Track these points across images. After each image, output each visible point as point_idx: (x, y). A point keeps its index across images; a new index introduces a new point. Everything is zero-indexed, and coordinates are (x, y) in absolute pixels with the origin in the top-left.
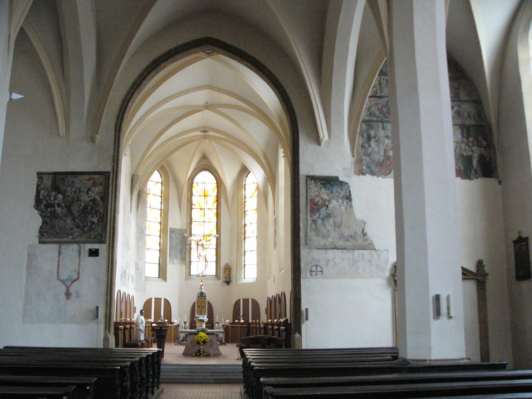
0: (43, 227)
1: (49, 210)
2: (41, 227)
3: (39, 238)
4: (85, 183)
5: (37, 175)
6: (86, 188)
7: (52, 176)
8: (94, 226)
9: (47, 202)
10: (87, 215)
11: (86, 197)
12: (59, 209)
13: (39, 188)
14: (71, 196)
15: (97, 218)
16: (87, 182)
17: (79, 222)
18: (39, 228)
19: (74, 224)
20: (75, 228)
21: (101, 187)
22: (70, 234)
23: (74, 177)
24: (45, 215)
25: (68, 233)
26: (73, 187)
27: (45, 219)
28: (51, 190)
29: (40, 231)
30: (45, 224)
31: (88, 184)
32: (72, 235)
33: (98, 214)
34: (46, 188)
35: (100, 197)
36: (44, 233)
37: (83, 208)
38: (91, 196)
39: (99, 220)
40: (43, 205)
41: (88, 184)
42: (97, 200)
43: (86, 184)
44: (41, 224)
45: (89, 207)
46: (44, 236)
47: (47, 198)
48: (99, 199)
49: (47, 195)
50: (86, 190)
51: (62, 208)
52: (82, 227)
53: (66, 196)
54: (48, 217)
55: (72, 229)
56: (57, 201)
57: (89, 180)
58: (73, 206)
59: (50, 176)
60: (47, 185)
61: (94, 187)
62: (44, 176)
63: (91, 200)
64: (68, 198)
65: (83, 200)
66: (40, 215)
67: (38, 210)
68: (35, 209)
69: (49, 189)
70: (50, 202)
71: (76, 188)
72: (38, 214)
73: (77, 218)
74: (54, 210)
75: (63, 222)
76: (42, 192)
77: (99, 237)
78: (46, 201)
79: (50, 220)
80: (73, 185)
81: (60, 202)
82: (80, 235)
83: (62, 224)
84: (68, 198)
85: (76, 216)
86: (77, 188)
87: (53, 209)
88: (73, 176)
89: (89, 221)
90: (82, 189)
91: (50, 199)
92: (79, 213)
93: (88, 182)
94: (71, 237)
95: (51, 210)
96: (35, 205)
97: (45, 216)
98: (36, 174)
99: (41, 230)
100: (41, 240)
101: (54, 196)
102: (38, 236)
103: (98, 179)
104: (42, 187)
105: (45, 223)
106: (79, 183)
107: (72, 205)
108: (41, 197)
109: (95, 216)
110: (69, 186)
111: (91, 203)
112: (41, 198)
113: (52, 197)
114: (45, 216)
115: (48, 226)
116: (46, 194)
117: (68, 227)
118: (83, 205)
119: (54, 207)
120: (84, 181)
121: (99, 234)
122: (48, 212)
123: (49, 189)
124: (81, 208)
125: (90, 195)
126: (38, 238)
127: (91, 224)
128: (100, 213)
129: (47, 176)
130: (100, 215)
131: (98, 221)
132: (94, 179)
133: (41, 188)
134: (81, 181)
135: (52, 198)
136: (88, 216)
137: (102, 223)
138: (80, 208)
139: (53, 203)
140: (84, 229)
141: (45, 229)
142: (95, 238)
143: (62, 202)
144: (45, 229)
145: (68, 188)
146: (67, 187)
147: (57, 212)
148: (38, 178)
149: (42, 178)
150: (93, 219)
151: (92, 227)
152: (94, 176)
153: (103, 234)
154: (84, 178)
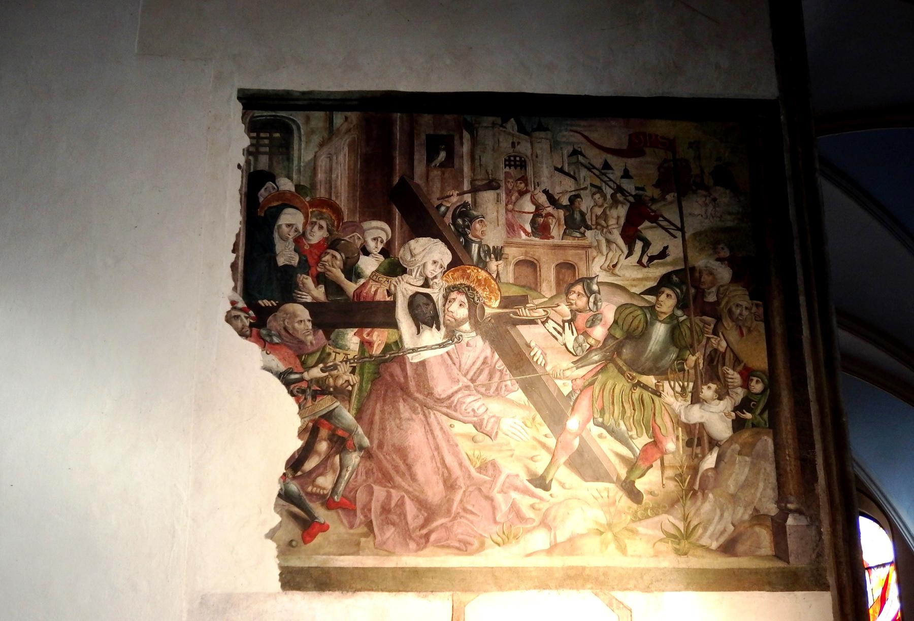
0: (310, 465)
1: (352, 339)
2: (295, 464)
3: (287, 549)
4: (607, 166)
5: (246, 107)
6: (615, 203)
7: (354, 116)
8: (710, 461)
9: (333, 287)
10: (651, 380)
11: (623, 262)
12: (432, 336)
13: (263, 194)
14: (513, 253)
15: (726, 405)
16: (618, 164)
17: (596, 431)
18: (282, 470)
19: (551, 442)
20: (563, 474)
21: (724, 197)
22: (529, 514)
23: (522, 130)
24: (318, 381)
25: (514, 509)
26: (522, 194)
27: (326, 404)
28: (352, 212)
29: (285, 496)
30: (323, 446)
31: (626, 175)
32: (545, 523)
33: (734, 377)
34: (322, 193)
35: (731, 262)
36: (321, 514)
37: (610, 336)
38: (663, 254)
39: (748, 416)
40: (304, 313)
41: (626, 175)
42: (706, 278)
43: (616, 174)
44: (297, 444)
45: (660, 331)
46: (324, 528)
47: (334, 265)
48: (724, 274)
49: (333, 243)
50: (621, 212)
51: (452, 336)
52: (623, 472)
53: (475, 248)
54: (341, 393)
55: (541, 482)
56: (406, 287)
57: (633, 150)
58: (532, 322)
59: (338, 119)
60: (321, 176)
61: (670, 197)
62: (298, 117)
63: (665, 281)
64: (493, 265)
65: (604, 277)
66: (283, 377)
67: (265, 343)
68: (242, 334)
69: (343, 201)
70: (351, 287)
71: (543, 199)
72: (267, 369)
73: (571, 401)
74: (387, 348)
75: (470, 429)
76: (291, 218)
77: (765, 536)
78: (320, 279)
79: (358, 417)
80: (524, 179)
81: (436, 293)
82: (610, 526)
83: (465, 447)
84: (493, 265)
85: (566, 391)
86: (553, 201)
87: (379, 338)
88: (512, 125)
89: (664, 422)
90: (585, 204)
91: (352, 272)
92: (582, 372)
93: (631, 163)
94: (539, 539)
95: (365, 345)
96: (241, 304)
97: (321, 389)
98: (240, 106)
99: (294, 487)
100: (296, 562)
101: (385, 252)
102: (271, 535)
103: (695, 145)
104: (286, 185)
105: (324, 433)
106: (561, 171)
107: (525, 313)
108: (286, 255)
109: (708, 392)
110: (492, 185)
111: (667, 303)
112: (281, 261)
113: (367, 253)
114: (321, 389)
115: (354, 459)
116: (317, 236)
117: (511, 468)
118: (609, 313)
119: (394, 325)
120: (596, 158)
121: (758, 517)
122: (346, 361)
123: (343, 201)
124: (599, 332)
125: (654, 250)
126: (271, 548)
127: (689, 444)
128: (747, 374)
129: (318, 118)
130: (746, 385)
131: (738, 425)
132: (669, 144)
133: (281, 195)
134: (575, 153)
135: (369, 265)
136: (657, 393)
137: (767, 442)
138: (586, 334)
139: (382, 296)
140: (640, 484)
141: (325, 482)
142: (728, 548)
143: (450, 290)
144: (325, 482)
145: (488, 197)
146: (474, 190)
147: (414, 358)
148: (253, 127)
149: (286, 129)
150: (696, 415)
151: (695, 469)
152: (661, 127)
153: (790, 521)
154: (594, 136)
